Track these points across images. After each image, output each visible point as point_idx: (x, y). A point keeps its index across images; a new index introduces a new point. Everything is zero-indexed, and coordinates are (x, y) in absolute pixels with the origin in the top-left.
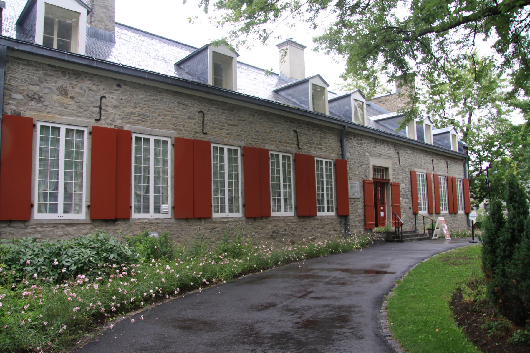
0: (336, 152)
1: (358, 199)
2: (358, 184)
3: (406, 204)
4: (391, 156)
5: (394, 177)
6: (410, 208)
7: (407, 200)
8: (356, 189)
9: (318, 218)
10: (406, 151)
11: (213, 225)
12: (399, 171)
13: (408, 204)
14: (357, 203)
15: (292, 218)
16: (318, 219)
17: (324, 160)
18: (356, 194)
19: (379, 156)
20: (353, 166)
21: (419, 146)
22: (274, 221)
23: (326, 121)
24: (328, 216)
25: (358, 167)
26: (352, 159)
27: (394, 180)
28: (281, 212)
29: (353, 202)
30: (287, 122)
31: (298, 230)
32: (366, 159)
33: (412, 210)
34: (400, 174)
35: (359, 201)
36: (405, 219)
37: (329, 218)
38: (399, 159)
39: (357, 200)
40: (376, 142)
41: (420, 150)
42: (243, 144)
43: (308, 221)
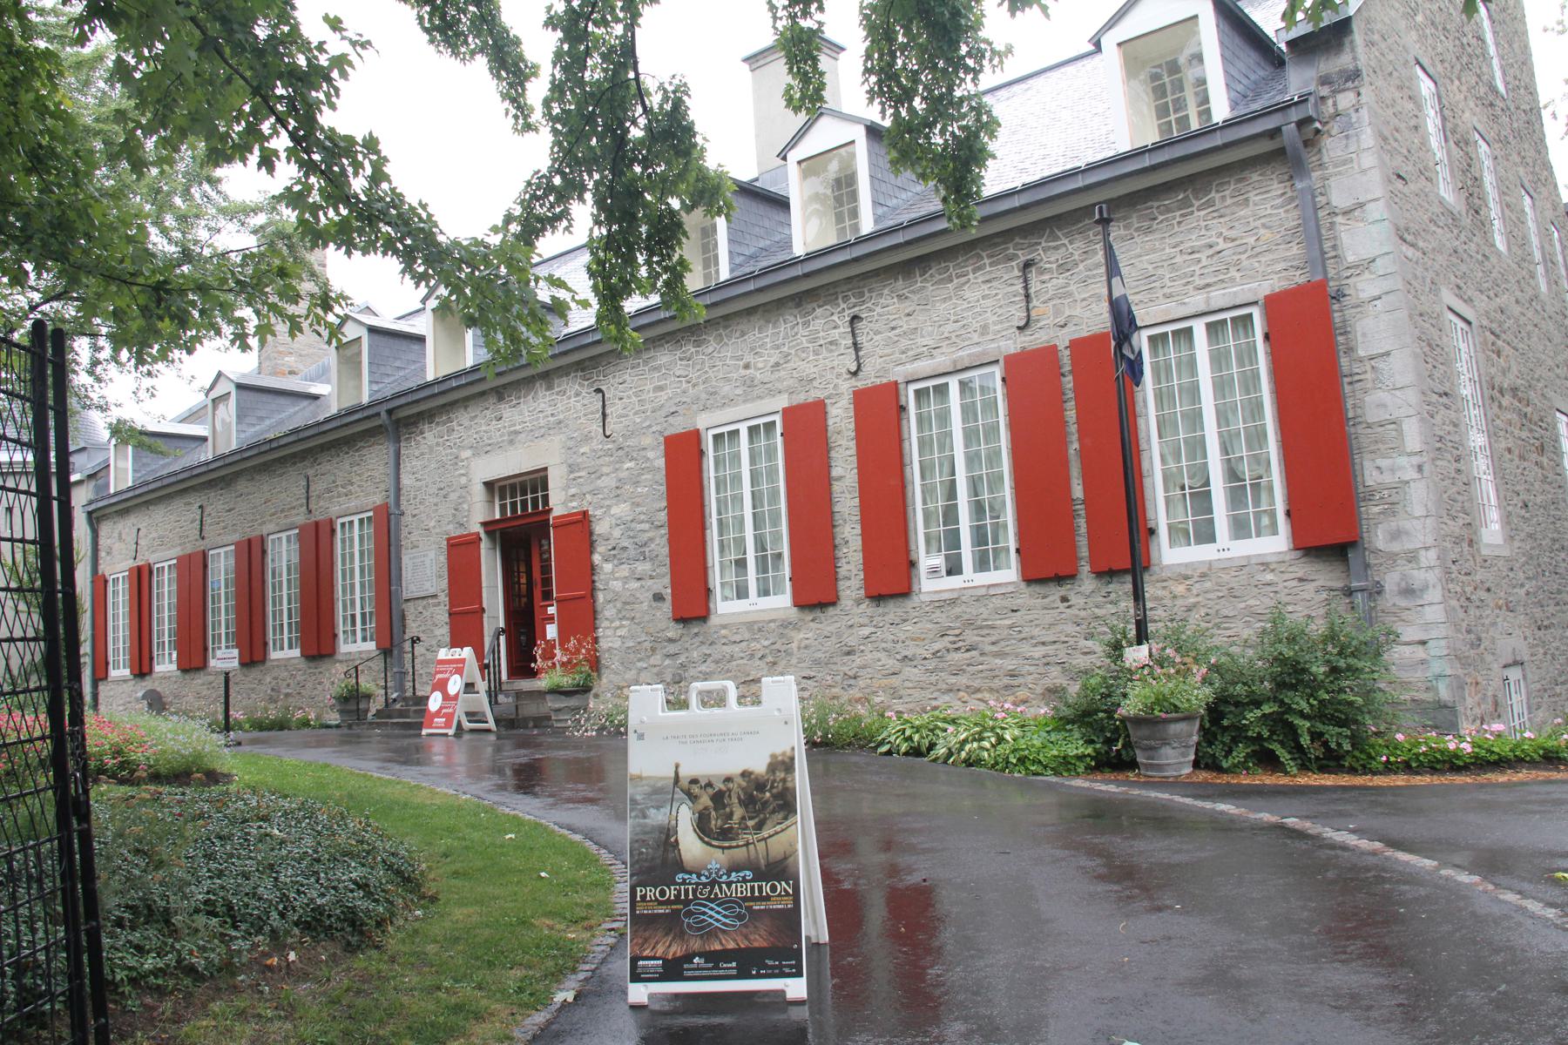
0: (383, 486)
1: (435, 596)
2: (432, 555)
3: (635, 585)
4: (560, 422)
5: (573, 491)
6: (658, 597)
7: (643, 567)
8: (428, 572)
9: (340, 658)
10: (646, 362)
11: (211, 678)
12: (601, 461)
13: (650, 582)
14: (431, 609)
15: (296, 661)
16: (341, 662)
17: (356, 519)
18: (428, 585)
19: (511, 442)
20: (422, 508)
21: (1023, 208)
22: (273, 667)
23: (300, 440)
24: (360, 652)
25: (436, 505)
26: (419, 489)
27: (574, 504)
28: (747, 597)
29: (420, 609)
30: (295, 463)
31: (309, 685)
32: (462, 472)
33: (667, 607)
34: (605, 470)
35: (439, 604)
36: (631, 644)
37: (363, 656)
38: (604, 415)
39: (431, 601)
40: (501, 398)
41: (750, 312)
42: (236, 537)
43: (324, 666)
